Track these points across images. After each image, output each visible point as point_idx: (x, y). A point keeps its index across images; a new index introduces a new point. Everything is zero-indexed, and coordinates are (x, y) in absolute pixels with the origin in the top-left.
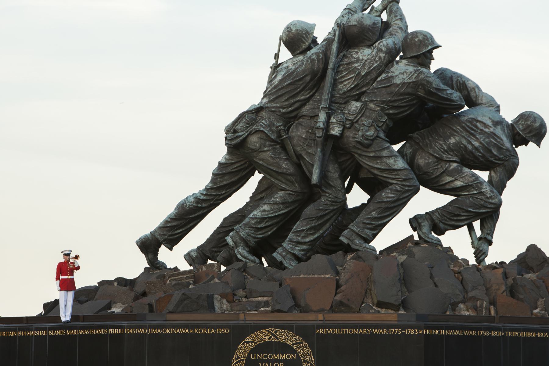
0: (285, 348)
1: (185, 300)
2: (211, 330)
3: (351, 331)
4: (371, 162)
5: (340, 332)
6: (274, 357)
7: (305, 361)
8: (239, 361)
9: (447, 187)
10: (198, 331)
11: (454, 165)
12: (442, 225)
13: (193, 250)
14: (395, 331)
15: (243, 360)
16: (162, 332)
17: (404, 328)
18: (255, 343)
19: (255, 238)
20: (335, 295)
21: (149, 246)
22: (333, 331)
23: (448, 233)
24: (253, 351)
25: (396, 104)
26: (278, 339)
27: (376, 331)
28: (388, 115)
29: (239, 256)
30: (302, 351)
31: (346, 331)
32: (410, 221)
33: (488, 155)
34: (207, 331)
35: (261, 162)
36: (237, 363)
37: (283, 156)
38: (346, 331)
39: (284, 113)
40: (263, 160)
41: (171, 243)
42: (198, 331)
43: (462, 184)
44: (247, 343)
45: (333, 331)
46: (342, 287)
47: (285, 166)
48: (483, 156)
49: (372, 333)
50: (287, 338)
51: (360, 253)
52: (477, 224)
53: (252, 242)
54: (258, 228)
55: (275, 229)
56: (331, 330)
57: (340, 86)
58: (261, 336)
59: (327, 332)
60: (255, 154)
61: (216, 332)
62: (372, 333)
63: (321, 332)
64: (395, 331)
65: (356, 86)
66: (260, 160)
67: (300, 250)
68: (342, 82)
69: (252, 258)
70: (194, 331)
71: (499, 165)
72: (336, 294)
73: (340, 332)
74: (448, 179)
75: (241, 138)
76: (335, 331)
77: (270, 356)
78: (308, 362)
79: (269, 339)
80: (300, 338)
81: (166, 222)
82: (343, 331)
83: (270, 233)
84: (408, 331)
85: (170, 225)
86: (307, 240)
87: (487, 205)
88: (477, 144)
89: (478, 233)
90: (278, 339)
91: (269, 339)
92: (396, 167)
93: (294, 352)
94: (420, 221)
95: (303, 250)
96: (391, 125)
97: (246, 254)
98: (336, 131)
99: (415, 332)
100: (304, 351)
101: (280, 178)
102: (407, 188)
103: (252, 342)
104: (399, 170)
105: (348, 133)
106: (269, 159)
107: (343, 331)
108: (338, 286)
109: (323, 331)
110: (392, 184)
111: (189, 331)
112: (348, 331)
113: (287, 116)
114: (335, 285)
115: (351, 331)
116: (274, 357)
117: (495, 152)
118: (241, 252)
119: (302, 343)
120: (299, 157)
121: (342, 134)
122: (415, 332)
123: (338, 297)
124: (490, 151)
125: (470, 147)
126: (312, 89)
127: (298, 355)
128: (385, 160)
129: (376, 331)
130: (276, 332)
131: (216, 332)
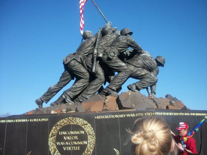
0: (78, 128)
1: (37, 111)
2: (38, 120)
3: (115, 116)
4: (113, 64)
5: (109, 117)
6: (72, 133)
7: (89, 135)
8: (53, 136)
9: (139, 75)
10: (32, 120)
11: (141, 68)
12: (139, 87)
13: (53, 103)
14: (139, 114)
15: (55, 135)
16: (14, 122)
17: (144, 112)
18: (62, 126)
19: (73, 95)
20: (104, 107)
21: (39, 103)
22: (104, 117)
23: (141, 90)
24: (61, 130)
25: (121, 46)
26: (74, 123)
27: (128, 115)
28: (118, 50)
29: (67, 101)
30: (87, 129)
31: (112, 116)
32: (128, 87)
33: (151, 66)
34: (36, 120)
35: (74, 70)
36: (52, 137)
37: (83, 67)
38: (112, 116)
39: (83, 54)
40: (75, 69)
41: (47, 101)
42: (32, 120)
43: (144, 73)
44: (58, 126)
45: (104, 117)
46: (106, 104)
47: (83, 70)
48: (150, 66)
49: (126, 116)
50: (80, 121)
51: (112, 94)
52: (149, 88)
53: (72, 96)
54: (74, 91)
55: (80, 92)
56: (103, 117)
57: (101, 44)
58: (65, 121)
59: (101, 118)
60: (73, 67)
61: (41, 120)
62: (126, 116)
63: (98, 117)
64: (139, 114)
65: (107, 43)
66: (74, 69)
67: (89, 97)
68: (102, 43)
69: (71, 101)
70: (30, 120)
71: (154, 69)
72: (104, 107)
73: (109, 117)
74: (139, 72)
75: (68, 62)
76: (106, 117)
77: (70, 133)
78: (91, 135)
79: (69, 123)
80: (86, 122)
81: (45, 94)
82: (110, 116)
83: (78, 93)
84: (146, 114)
85: (46, 94)
86: (91, 93)
87: (153, 80)
88: (147, 62)
89: (150, 91)
90: (74, 123)
91: (69, 123)
92: (122, 65)
93: (83, 130)
94: (132, 86)
95: (90, 97)
96: (119, 54)
97: (69, 100)
98: (101, 55)
99: (150, 114)
100: (89, 129)
101: (81, 74)
102: (127, 72)
103: (60, 125)
104: (124, 66)
105: (105, 56)
106: (78, 68)
107: (110, 116)
108: (105, 104)
109: (99, 117)
110: (121, 71)
111: (27, 120)
112: (113, 117)
113: (84, 55)
114: (103, 104)
115: (115, 116)
116: (72, 133)
117: (153, 65)
118: (68, 100)
119: (87, 124)
120: (88, 67)
121: (102, 57)
122: (150, 114)
123: (105, 108)
124: (152, 65)
125: (145, 63)
126: (92, 47)
127: (85, 131)
128: (118, 63)
129: (128, 115)
130: (73, 119)
131: (41, 120)
